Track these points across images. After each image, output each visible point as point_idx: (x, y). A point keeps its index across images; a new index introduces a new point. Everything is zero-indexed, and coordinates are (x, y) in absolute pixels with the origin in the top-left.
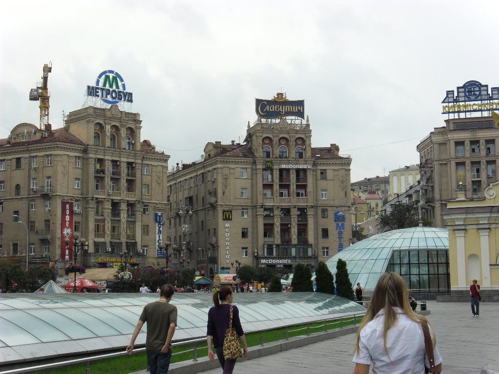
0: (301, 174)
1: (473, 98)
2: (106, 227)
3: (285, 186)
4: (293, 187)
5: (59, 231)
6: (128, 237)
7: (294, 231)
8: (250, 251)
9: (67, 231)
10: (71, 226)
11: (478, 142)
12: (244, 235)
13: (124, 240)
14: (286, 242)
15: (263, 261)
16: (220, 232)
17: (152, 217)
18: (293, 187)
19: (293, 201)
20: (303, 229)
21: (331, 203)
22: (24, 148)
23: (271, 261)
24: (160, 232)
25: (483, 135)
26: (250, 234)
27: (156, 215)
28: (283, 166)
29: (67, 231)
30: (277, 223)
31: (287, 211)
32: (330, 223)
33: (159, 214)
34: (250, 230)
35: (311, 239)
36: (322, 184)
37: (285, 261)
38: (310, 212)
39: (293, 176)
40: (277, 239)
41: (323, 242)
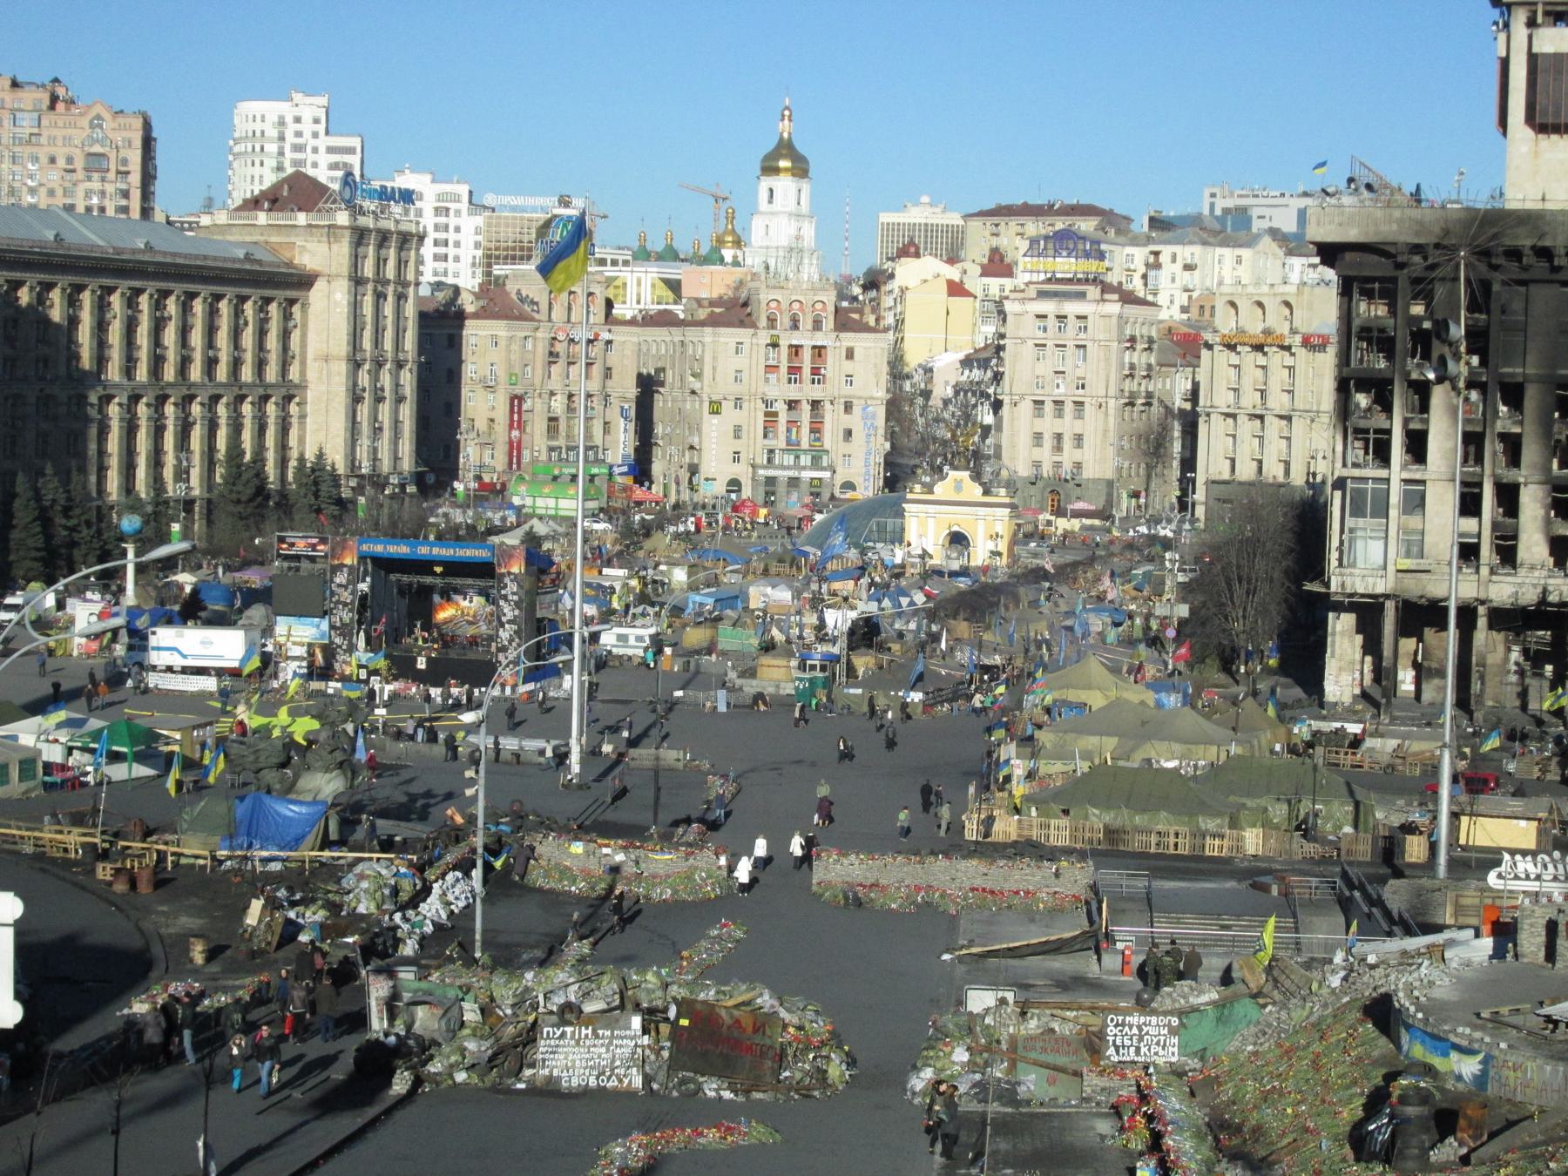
0: (819, 351)
1: (1065, 253)
3: (794, 370)
4: (807, 371)
7: (805, 430)
12: (737, 437)
14: (793, 446)
15: (761, 472)
16: (705, 428)
18: (807, 371)
19: (806, 391)
20: (816, 429)
21: (859, 394)
23: (771, 473)
25: (1072, 308)
26: (744, 434)
28: (795, 342)
30: (783, 418)
31: (792, 405)
32: (855, 421)
34: (745, 428)
35: (828, 442)
36: (848, 367)
38: (827, 406)
39: (807, 355)
40: (781, 442)
41: (844, 448)
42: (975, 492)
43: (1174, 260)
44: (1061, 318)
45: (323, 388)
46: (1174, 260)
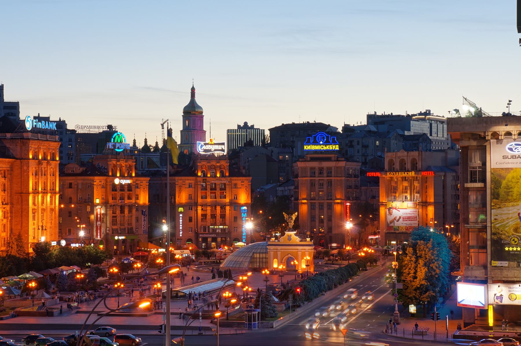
2: (118, 220)
5: (95, 223)
6: (128, 224)
8: (193, 229)
9: (99, 223)
10: (100, 220)
11: (323, 168)
13: (126, 226)
17: (140, 212)
22: (74, 178)
23: (205, 236)
24: (144, 220)
27: (142, 211)
29: (99, 223)
33: (144, 210)
35: (227, 222)
37: (213, 236)
42: (296, 239)
43: (358, 144)
44: (321, 170)
45: (19, 207)
46: (358, 144)
